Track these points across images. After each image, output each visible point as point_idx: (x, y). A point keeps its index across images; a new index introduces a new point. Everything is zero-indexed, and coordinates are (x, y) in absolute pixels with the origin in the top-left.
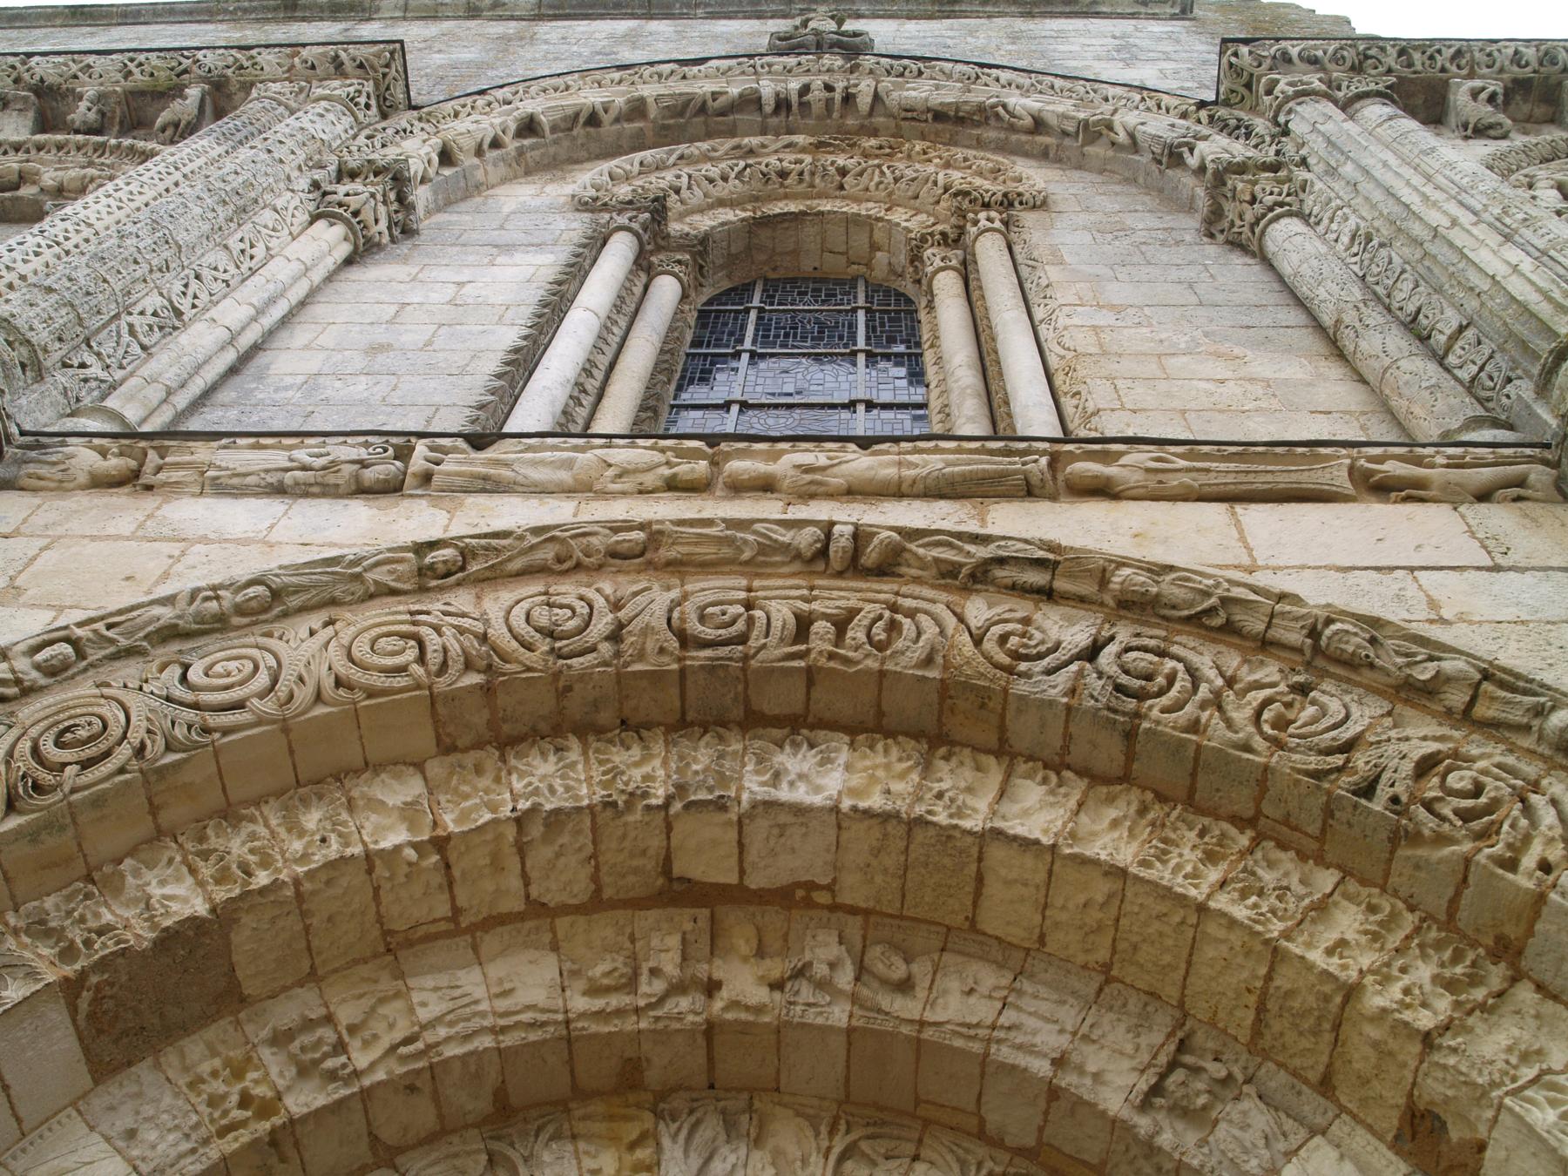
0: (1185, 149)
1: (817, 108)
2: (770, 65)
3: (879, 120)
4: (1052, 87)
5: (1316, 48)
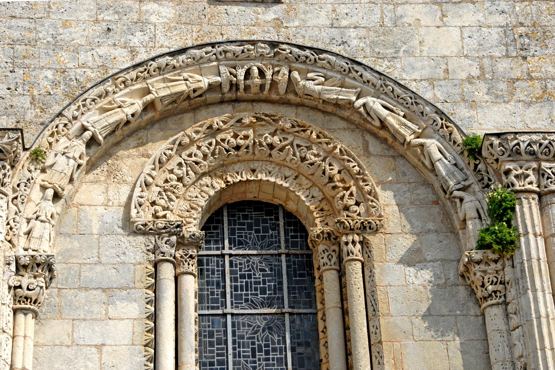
0: (458, 201)
1: (254, 90)
2: (225, 52)
3: (291, 97)
4: (393, 91)
5: (535, 143)
